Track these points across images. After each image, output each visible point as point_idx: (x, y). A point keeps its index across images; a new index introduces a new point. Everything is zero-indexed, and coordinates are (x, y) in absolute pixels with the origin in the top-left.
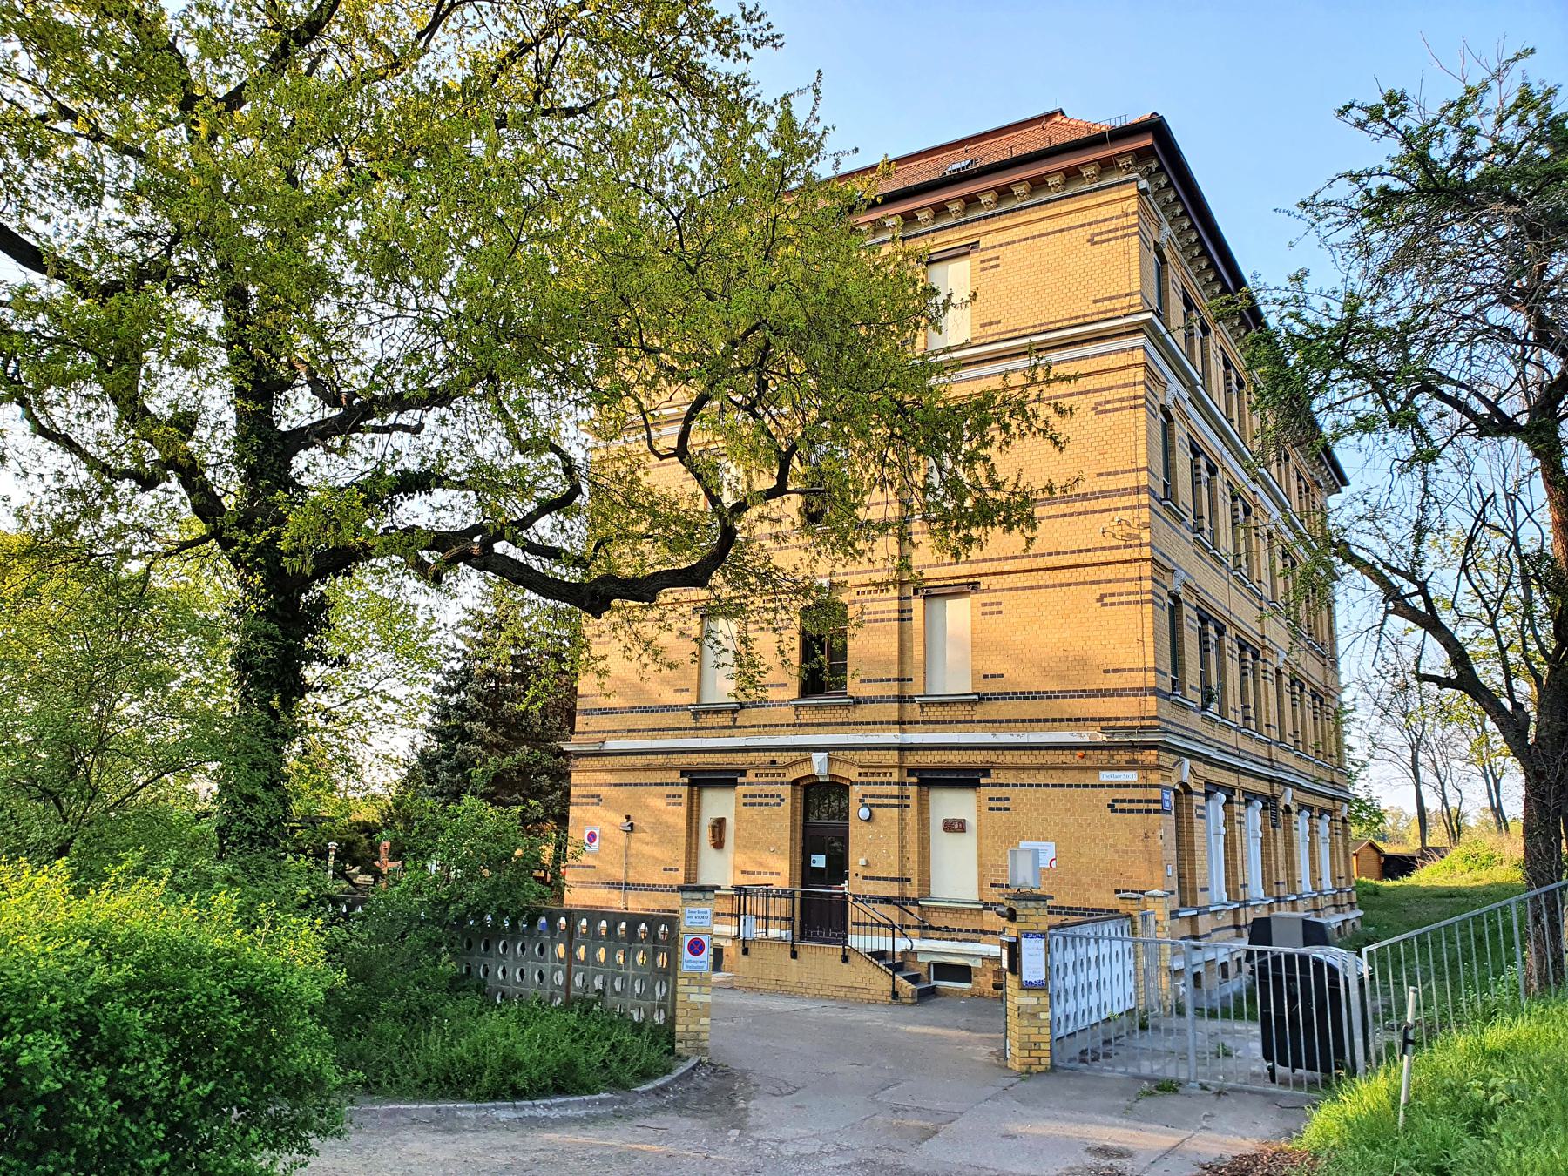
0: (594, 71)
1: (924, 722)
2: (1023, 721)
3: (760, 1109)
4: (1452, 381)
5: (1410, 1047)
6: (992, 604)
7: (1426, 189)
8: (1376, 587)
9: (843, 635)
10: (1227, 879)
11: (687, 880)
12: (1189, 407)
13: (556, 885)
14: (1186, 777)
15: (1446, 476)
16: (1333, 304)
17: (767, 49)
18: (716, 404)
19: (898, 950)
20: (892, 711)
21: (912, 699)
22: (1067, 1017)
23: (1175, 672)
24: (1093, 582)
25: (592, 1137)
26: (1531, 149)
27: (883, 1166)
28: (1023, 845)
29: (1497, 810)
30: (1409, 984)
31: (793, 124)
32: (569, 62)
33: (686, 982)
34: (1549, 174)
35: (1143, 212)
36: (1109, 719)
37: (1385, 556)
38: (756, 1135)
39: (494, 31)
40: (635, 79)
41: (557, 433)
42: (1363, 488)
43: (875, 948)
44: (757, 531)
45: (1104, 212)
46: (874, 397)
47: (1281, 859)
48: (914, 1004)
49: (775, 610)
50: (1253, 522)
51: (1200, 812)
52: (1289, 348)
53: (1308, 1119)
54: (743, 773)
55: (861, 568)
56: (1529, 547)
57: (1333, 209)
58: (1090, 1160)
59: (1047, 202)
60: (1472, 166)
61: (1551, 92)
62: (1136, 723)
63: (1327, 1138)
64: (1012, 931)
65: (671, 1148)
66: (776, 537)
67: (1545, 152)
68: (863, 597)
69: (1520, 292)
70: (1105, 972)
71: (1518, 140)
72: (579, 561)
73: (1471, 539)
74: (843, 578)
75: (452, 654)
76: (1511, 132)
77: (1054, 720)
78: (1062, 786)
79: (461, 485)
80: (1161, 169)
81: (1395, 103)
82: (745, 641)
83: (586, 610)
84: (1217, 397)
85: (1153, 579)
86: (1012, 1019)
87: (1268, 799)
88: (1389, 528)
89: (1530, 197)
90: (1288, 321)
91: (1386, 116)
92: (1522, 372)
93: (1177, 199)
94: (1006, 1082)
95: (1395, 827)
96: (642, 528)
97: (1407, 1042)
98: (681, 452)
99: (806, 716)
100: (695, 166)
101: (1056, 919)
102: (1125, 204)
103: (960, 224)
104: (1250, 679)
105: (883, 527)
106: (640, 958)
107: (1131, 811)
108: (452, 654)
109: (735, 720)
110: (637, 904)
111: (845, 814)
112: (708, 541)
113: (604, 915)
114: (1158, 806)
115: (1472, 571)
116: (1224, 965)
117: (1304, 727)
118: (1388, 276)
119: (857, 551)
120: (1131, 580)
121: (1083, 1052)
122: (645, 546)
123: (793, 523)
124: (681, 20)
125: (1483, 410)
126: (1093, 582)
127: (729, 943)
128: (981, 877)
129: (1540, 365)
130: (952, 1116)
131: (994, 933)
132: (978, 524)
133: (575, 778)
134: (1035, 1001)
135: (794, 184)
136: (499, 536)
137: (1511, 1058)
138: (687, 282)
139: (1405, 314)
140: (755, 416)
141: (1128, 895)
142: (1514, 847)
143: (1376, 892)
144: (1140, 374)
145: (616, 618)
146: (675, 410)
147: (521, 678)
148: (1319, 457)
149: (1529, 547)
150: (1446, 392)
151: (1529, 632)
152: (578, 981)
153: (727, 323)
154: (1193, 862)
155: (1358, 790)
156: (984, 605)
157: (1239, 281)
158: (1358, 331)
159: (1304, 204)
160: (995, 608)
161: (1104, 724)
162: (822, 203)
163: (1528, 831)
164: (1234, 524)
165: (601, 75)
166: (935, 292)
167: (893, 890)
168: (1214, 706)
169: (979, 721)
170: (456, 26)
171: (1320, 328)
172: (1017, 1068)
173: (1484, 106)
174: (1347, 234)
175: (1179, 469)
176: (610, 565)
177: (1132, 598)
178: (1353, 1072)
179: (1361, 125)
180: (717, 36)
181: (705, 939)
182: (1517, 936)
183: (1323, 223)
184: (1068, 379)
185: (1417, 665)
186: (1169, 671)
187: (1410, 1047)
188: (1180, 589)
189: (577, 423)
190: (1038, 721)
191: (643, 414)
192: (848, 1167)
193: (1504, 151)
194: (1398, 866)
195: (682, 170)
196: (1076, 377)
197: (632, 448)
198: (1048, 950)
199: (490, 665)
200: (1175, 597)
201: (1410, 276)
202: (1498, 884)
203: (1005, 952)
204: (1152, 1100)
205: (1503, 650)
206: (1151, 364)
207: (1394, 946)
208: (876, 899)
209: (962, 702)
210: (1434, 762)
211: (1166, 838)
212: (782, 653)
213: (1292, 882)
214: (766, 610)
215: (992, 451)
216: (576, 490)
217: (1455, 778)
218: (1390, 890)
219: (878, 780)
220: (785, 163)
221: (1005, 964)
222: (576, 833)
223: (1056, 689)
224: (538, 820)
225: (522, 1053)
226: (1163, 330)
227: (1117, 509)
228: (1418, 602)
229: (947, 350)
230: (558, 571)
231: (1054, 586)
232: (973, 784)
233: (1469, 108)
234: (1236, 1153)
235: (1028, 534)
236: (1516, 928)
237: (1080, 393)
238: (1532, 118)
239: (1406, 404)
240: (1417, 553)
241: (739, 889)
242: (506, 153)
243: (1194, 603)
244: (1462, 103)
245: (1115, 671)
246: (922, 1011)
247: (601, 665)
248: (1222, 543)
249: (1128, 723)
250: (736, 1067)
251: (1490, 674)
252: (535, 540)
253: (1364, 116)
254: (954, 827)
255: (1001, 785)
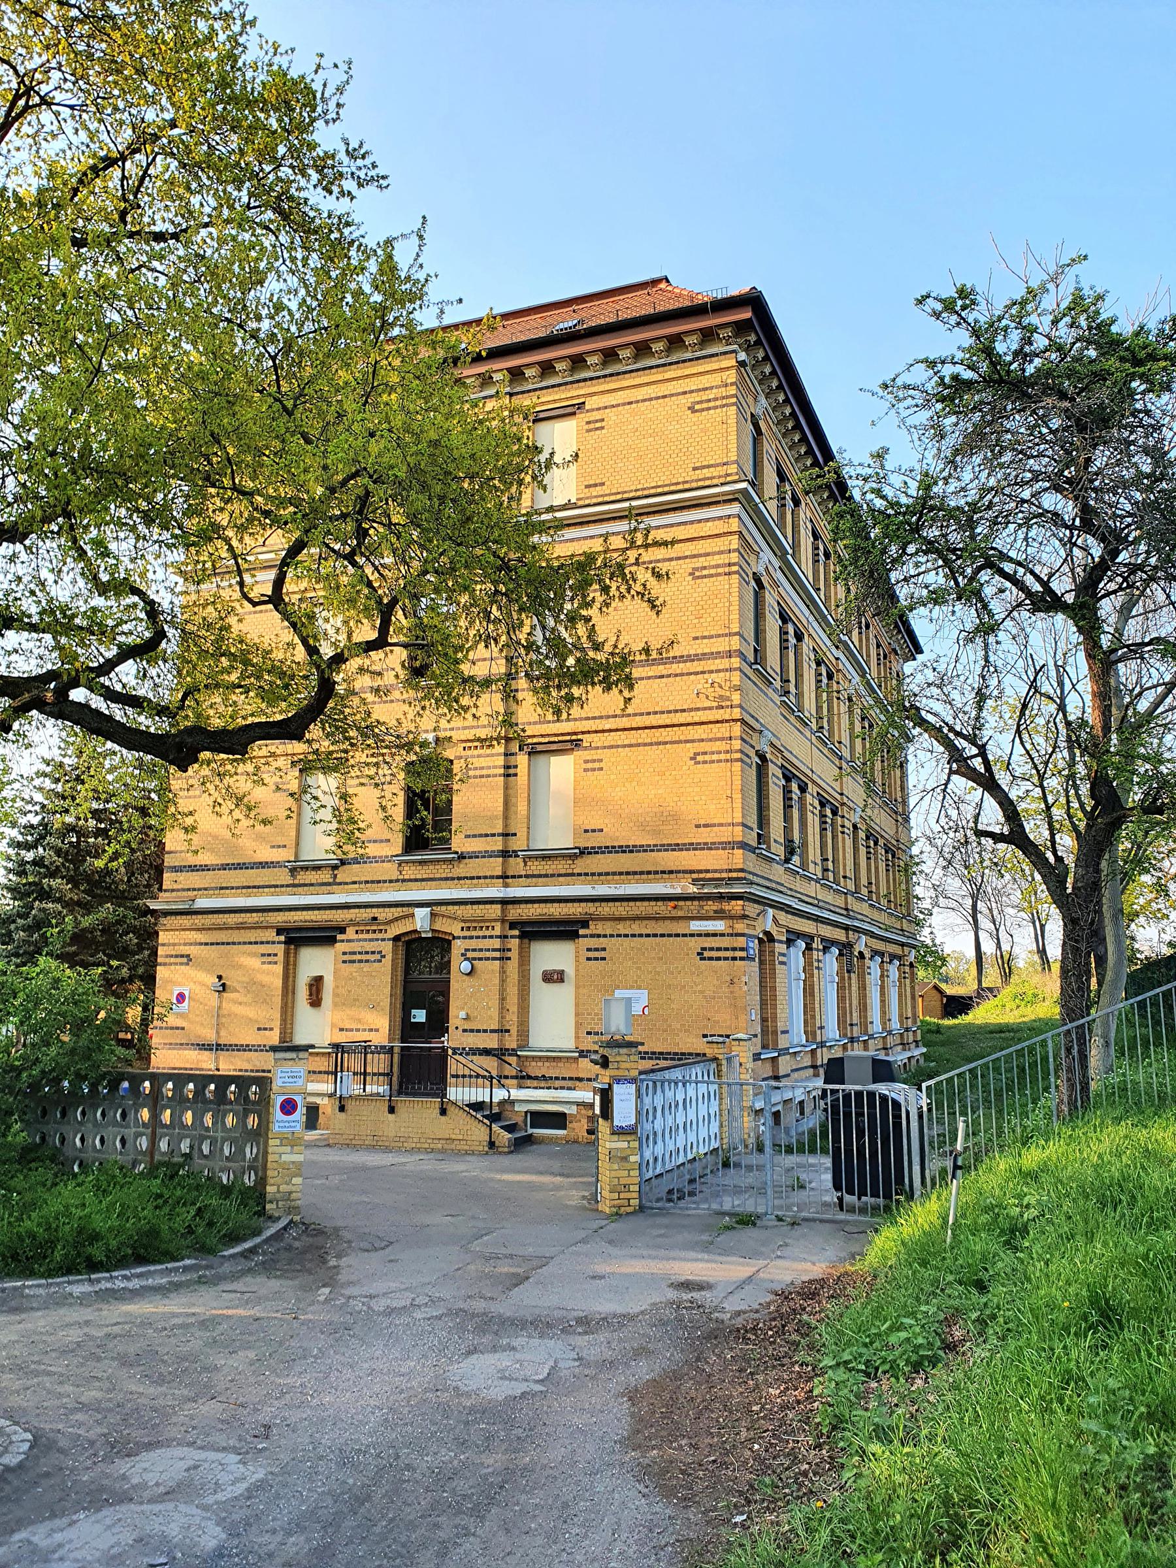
0: (187, 195)
1: (527, 876)
2: (621, 874)
3: (352, 1265)
4: (1011, 560)
5: (959, 1172)
6: (594, 761)
7: (992, 380)
8: (942, 749)
9: (449, 790)
10: (806, 1022)
11: (282, 1040)
12: (779, 576)
13: (143, 1051)
14: (769, 926)
15: (1005, 645)
16: (911, 482)
17: (371, 189)
18: (315, 551)
19: (495, 1100)
20: (495, 866)
21: (515, 854)
22: (656, 1159)
23: (760, 827)
24: (687, 741)
25: (174, 1306)
26: (1082, 349)
27: (473, 1315)
28: (618, 994)
29: (1042, 952)
30: (961, 1115)
31: (394, 269)
32: (159, 183)
33: (278, 1142)
34: (1095, 374)
35: (741, 383)
36: (700, 872)
37: (951, 721)
38: (347, 1292)
39: (74, 139)
40: (231, 208)
41: (143, 575)
42: (933, 656)
43: (473, 1099)
44: (357, 685)
45: (705, 381)
46: (478, 551)
47: (855, 1002)
48: (512, 1152)
49: (377, 765)
50: (835, 687)
51: (781, 959)
52: (870, 522)
53: (870, 1243)
54: (342, 930)
55: (467, 724)
56: (1073, 714)
57: (911, 392)
58: (672, 1294)
59: (651, 368)
60: (1031, 361)
61: (1100, 297)
62: (724, 875)
63: (885, 1258)
64: (605, 1077)
65: (256, 1312)
66: (377, 691)
67: (1092, 353)
68: (469, 753)
69: (1069, 481)
70: (692, 1115)
71: (1070, 340)
72: (162, 711)
73: (1025, 706)
74: (448, 734)
75: (29, 807)
76: (1064, 333)
77: (649, 873)
78: (655, 935)
79: (33, 628)
80: (758, 343)
81: (966, 297)
82: (344, 797)
83: (171, 763)
84: (805, 567)
85: (743, 739)
86: (604, 1164)
87: (844, 945)
88: (955, 695)
89: (1078, 394)
90: (869, 496)
91: (958, 308)
92: (1070, 554)
93: (774, 373)
94: (596, 1225)
95: (956, 971)
96: (234, 677)
97: (956, 1167)
98: (276, 599)
99: (410, 872)
100: (293, 305)
101: (648, 1064)
102: (725, 375)
103: (566, 384)
104: (829, 834)
105: (487, 683)
106: (230, 1120)
107: (718, 959)
108: (29, 807)
109: (335, 876)
110: (229, 1065)
111: (446, 966)
112: (304, 695)
113: (211, 1078)
114: (743, 954)
115: (1025, 736)
116: (801, 1103)
117: (877, 877)
118: (958, 458)
119: (462, 707)
120: (722, 739)
121: (670, 1192)
122: (238, 697)
123: (397, 676)
124: (282, 150)
125: (1037, 587)
126: (687, 741)
127: (326, 1100)
128: (578, 1025)
129: (1085, 549)
130: (545, 1261)
131: (589, 1080)
132: (579, 683)
133: (163, 937)
134: (625, 1145)
135: (396, 331)
136: (75, 684)
137: (1044, 1178)
138: (282, 422)
139: (972, 495)
140: (354, 564)
141: (715, 1039)
142: (1052, 985)
143: (938, 1030)
144: (735, 542)
145: (206, 771)
146: (272, 556)
147: (103, 833)
148: (896, 626)
149: (1073, 714)
150: (1006, 569)
151: (1072, 792)
152: (163, 1146)
153: (325, 468)
154: (774, 1006)
155: (925, 936)
156: (586, 762)
157: (828, 455)
158: (932, 508)
159: (885, 386)
160: (596, 765)
161: (695, 876)
162: (424, 353)
163: (1064, 972)
164: (817, 688)
165: (195, 200)
166: (537, 450)
167: (492, 1042)
168: (796, 859)
169: (579, 875)
170: (31, 131)
171: (898, 504)
172: (607, 1210)
173: (1042, 306)
174: (923, 416)
175: (769, 635)
176: (199, 716)
177: (723, 756)
178: (910, 1197)
179: (937, 315)
180: (320, 170)
181: (298, 1099)
182: (1052, 1067)
183: (901, 405)
184: (665, 544)
185: (976, 822)
186: (755, 826)
187: (959, 1172)
188: (767, 749)
189: (166, 565)
190: (635, 873)
191: (235, 557)
192: (439, 1318)
193: (1058, 350)
194: (957, 1005)
195: (279, 307)
196: (673, 543)
197: (225, 594)
198: (639, 1095)
199: (69, 819)
200: (762, 757)
201: (977, 459)
202: (1040, 1019)
203: (598, 1098)
204: (733, 1233)
205: (1048, 808)
206: (745, 532)
207: (950, 1080)
208: (475, 1051)
209: (564, 856)
210: (991, 910)
211: (751, 984)
212: (384, 808)
213: (865, 1024)
214: (368, 764)
215: (593, 612)
216: (160, 635)
217: (1008, 924)
218: (950, 1027)
219: (481, 933)
220: (385, 308)
221: (597, 1111)
222: (163, 993)
223: (652, 843)
224: (123, 981)
225: (99, 1223)
226: (757, 500)
227: (711, 672)
228: (977, 763)
229: (551, 509)
230: (144, 722)
231: (651, 744)
232: (572, 936)
233: (1029, 307)
234: (806, 1278)
235: (626, 694)
236: (1051, 1060)
237: (679, 558)
238: (1083, 321)
239: (972, 579)
240: (977, 718)
241: (336, 1046)
242: (85, 272)
243: (780, 762)
244: (1023, 303)
245: (706, 826)
246: (518, 1159)
247: (189, 821)
248: (806, 706)
249: (717, 875)
250: (328, 1224)
251: (1037, 831)
252: (118, 688)
253: (939, 307)
254: (554, 977)
255: (599, 936)
